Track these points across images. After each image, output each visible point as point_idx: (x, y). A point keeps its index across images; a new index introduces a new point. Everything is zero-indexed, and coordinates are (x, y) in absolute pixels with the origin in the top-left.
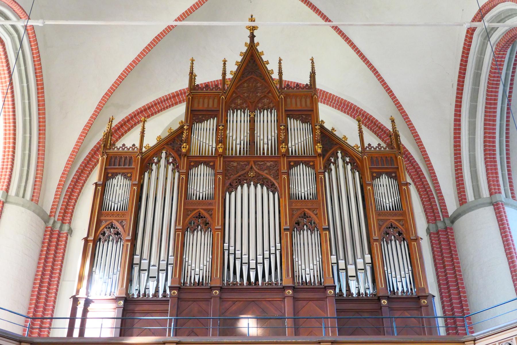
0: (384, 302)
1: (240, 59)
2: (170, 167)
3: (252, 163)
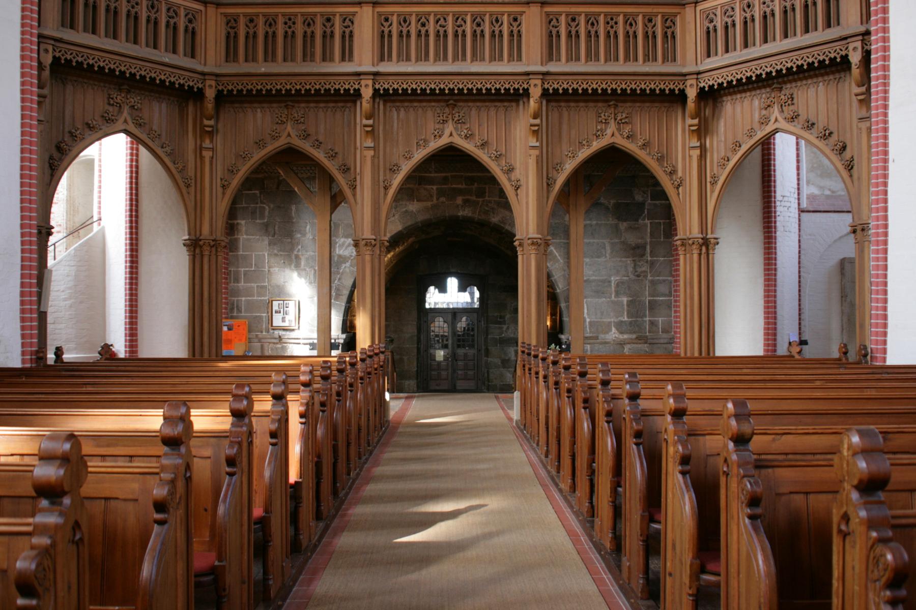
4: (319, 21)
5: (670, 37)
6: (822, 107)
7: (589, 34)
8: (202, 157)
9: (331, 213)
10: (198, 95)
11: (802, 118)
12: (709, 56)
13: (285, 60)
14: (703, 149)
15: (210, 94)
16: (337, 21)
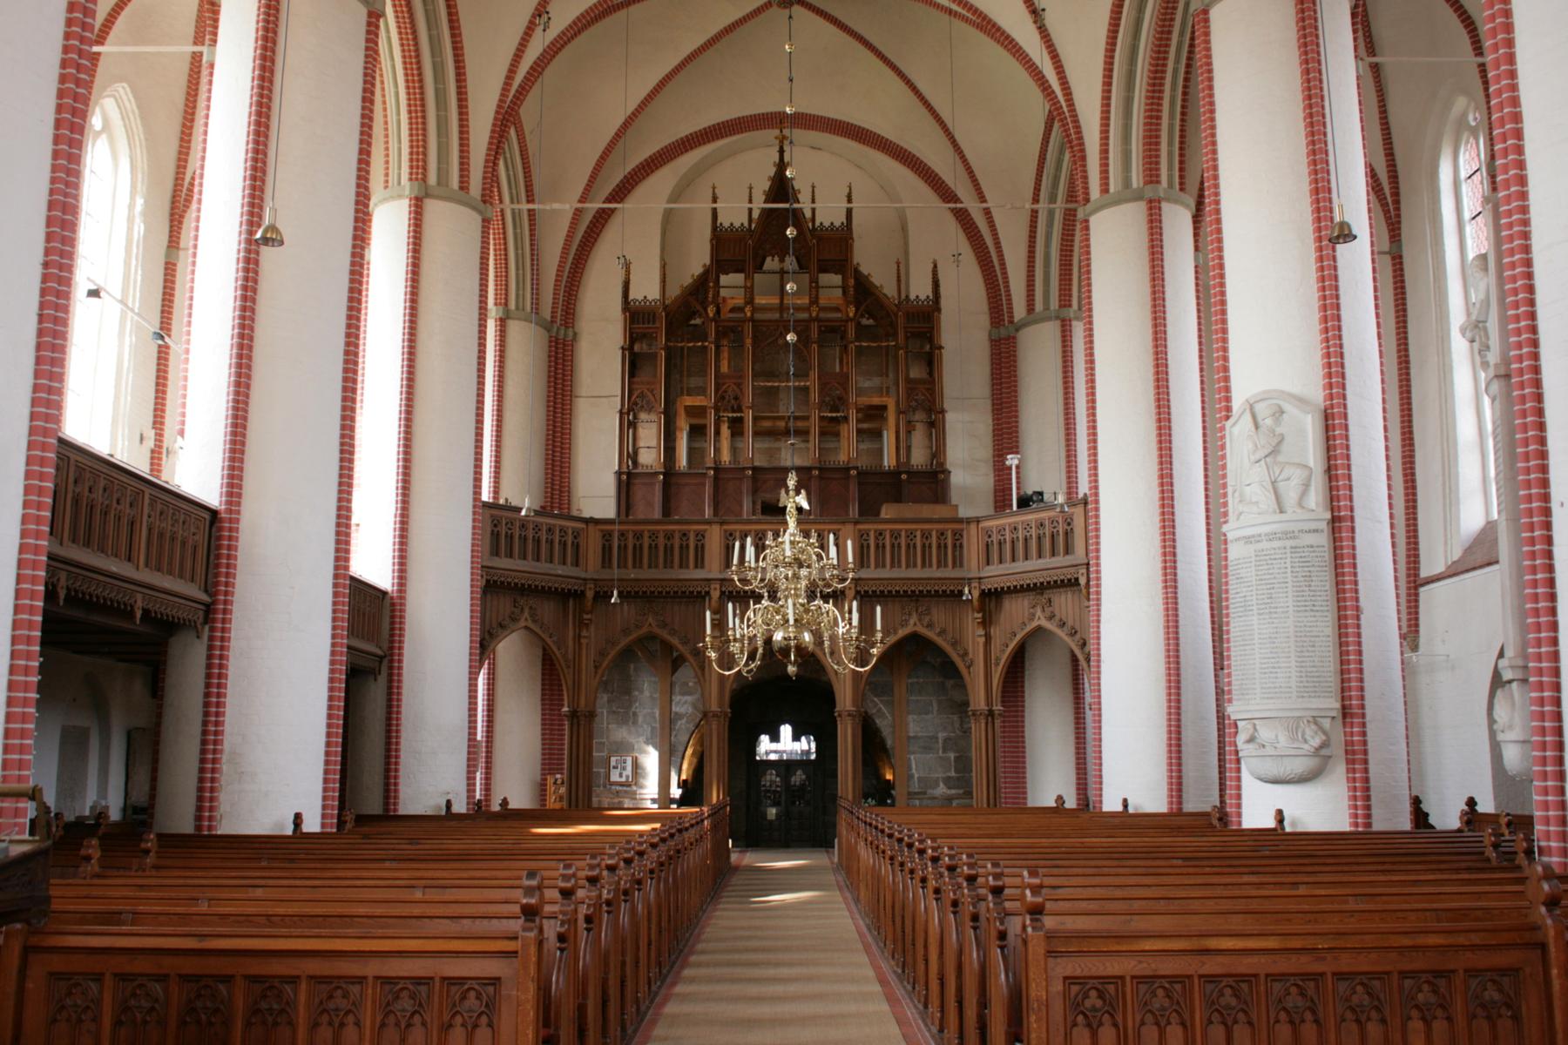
4: (677, 536)
5: (958, 546)
6: (1070, 612)
7: (893, 546)
8: (580, 644)
9: (673, 673)
10: (579, 596)
11: (1057, 618)
12: (988, 564)
13: (650, 567)
14: (988, 637)
15: (590, 594)
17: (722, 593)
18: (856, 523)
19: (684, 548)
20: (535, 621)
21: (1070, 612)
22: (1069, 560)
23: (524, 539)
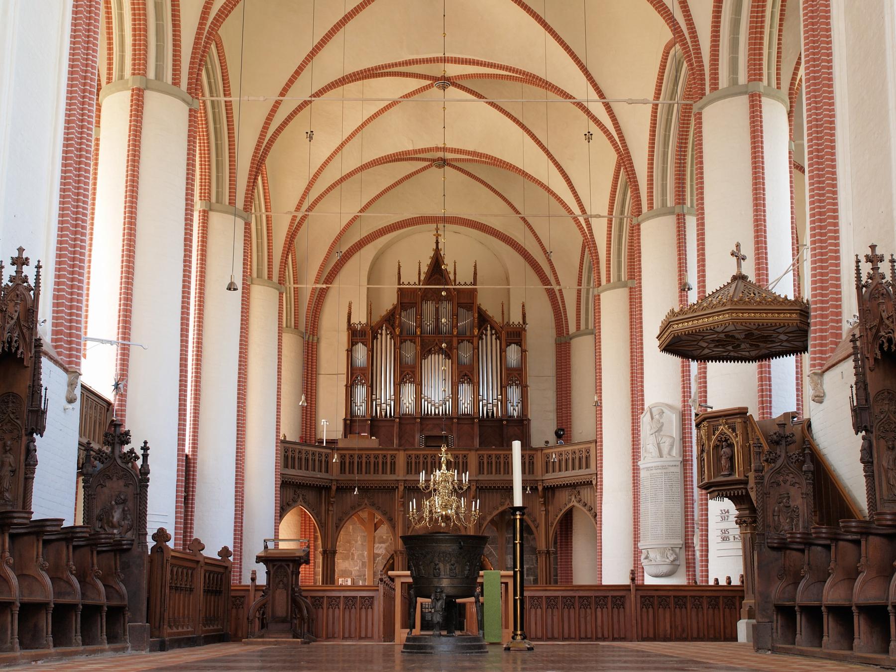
0: (505, 422)
1: (429, 261)
2: (389, 337)
3: (437, 341)
4: (381, 457)
6: (589, 498)
10: (328, 489)
11: (583, 501)
13: (366, 473)
14: (547, 511)
15: (334, 488)
16: (389, 457)
17: (405, 487)
18: (477, 450)
19: (384, 464)
20: (305, 502)
21: (589, 498)
22: (588, 471)
23: (300, 459)
